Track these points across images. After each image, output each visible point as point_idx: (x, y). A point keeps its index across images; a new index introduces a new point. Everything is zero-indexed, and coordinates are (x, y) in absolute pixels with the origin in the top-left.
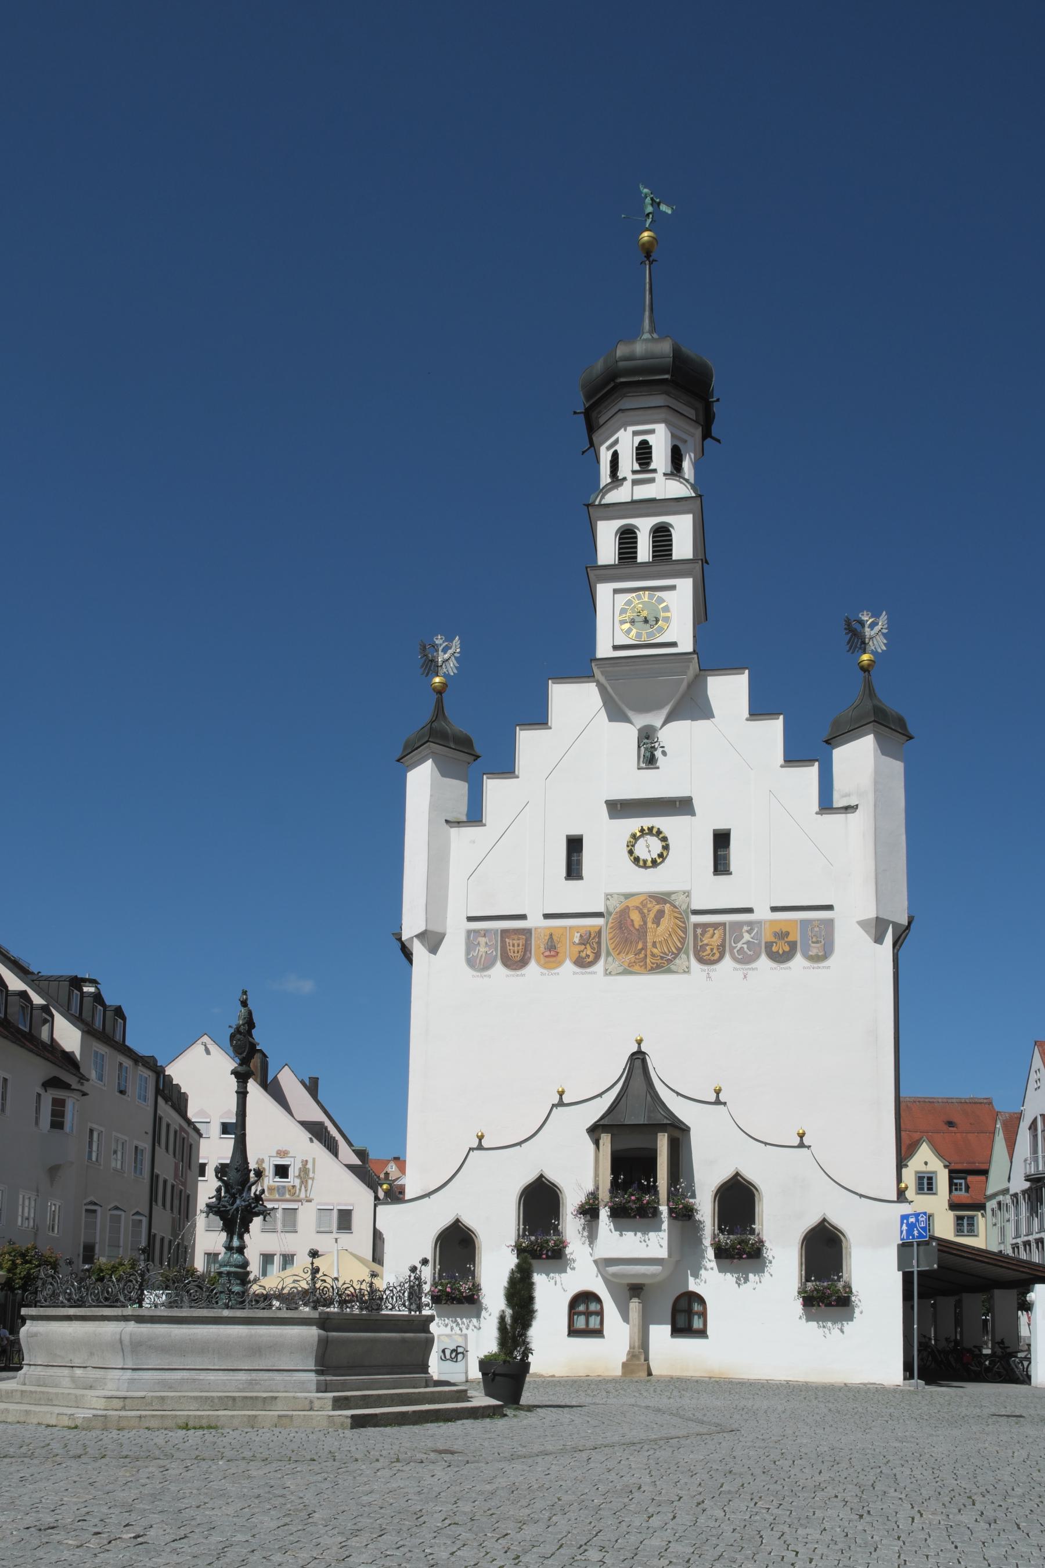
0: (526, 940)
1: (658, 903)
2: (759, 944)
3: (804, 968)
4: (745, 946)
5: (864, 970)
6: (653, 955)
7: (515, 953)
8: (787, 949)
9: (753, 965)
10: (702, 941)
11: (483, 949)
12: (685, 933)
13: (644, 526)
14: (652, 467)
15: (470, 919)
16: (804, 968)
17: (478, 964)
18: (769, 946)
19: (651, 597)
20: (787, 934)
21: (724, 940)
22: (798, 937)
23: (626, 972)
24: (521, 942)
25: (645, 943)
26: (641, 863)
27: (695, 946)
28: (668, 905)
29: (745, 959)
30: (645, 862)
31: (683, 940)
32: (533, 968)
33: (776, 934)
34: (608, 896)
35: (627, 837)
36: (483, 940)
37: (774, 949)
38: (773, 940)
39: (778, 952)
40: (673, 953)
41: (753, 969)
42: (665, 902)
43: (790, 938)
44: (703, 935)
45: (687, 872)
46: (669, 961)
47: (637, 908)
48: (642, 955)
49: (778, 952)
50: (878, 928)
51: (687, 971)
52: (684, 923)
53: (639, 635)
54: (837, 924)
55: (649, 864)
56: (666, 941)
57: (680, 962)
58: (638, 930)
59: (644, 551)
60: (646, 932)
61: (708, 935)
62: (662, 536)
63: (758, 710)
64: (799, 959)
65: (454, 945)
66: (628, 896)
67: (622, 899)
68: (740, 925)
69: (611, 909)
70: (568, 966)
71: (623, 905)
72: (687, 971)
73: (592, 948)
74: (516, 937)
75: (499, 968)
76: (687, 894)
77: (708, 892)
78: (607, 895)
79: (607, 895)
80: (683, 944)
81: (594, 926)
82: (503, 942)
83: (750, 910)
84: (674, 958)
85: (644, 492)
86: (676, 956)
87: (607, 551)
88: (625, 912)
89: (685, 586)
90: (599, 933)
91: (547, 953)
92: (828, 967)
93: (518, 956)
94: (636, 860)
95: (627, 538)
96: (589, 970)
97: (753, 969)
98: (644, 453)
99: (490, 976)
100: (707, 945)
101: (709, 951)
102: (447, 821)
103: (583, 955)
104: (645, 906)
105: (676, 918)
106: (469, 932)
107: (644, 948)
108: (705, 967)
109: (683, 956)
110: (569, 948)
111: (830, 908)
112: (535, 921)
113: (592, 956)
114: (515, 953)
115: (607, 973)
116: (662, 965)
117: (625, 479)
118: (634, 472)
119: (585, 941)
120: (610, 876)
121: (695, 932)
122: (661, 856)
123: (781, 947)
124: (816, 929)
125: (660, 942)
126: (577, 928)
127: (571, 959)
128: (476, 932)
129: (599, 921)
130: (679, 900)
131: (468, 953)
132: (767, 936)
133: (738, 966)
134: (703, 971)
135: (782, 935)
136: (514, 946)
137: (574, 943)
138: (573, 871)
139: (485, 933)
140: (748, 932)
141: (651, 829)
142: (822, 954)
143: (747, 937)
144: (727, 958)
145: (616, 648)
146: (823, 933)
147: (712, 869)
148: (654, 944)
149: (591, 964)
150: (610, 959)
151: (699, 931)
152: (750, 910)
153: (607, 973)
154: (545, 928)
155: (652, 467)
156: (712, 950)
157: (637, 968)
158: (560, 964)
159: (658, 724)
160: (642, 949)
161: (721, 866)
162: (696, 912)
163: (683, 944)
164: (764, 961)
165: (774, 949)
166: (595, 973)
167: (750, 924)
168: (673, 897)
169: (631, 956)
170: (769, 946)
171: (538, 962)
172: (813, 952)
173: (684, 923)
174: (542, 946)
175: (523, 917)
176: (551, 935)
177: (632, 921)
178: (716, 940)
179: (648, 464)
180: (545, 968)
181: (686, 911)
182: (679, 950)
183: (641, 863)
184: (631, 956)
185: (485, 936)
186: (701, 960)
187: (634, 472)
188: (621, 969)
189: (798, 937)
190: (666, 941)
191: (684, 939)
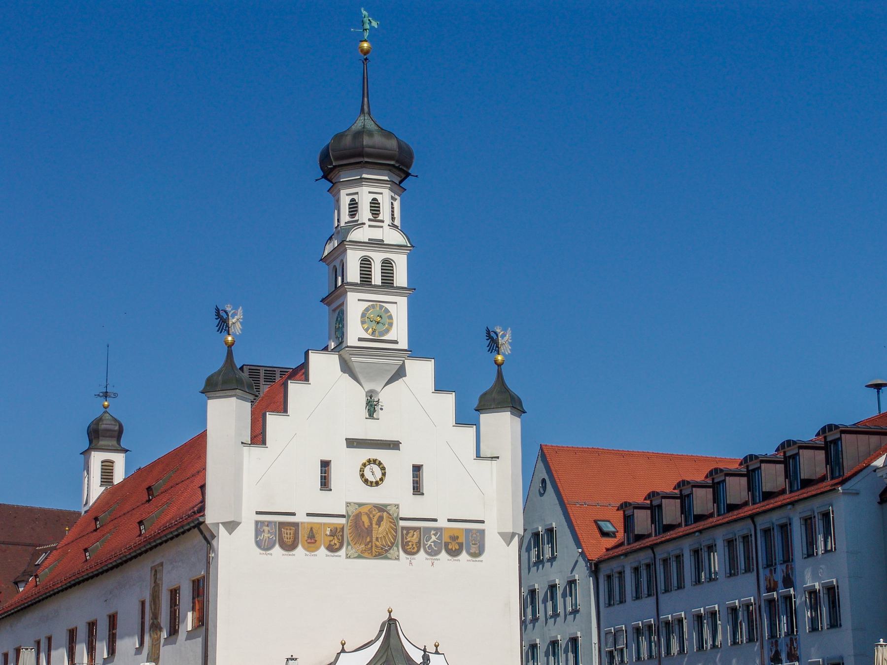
5: (502, 562)
6: (376, 546)
7: (288, 540)
8: (457, 547)
11: (266, 535)
12: (396, 532)
13: (377, 257)
15: (257, 513)
17: (264, 546)
18: (446, 544)
20: (458, 537)
22: (464, 542)
23: (359, 557)
24: (292, 532)
29: (433, 553)
30: (372, 482)
31: (395, 538)
32: (300, 550)
33: (451, 537)
34: (348, 504)
35: (359, 466)
37: (450, 547)
38: (449, 541)
42: (384, 511)
43: (459, 541)
44: (407, 534)
45: (395, 492)
46: (387, 551)
50: (508, 538)
51: (397, 559)
61: (410, 535)
62: (387, 265)
63: (439, 388)
64: (464, 555)
65: (246, 531)
66: (360, 505)
68: (428, 530)
69: (350, 513)
70: (323, 551)
72: (397, 559)
76: (397, 506)
78: (347, 503)
79: (347, 503)
83: (435, 520)
85: (376, 234)
88: (358, 516)
89: (402, 302)
90: (343, 529)
94: (366, 481)
95: (366, 263)
96: (336, 554)
98: (375, 206)
103: (332, 543)
104: (371, 512)
106: (257, 522)
107: (371, 541)
109: (395, 548)
110: (323, 536)
111: (483, 522)
113: (338, 544)
114: (288, 540)
116: (382, 553)
117: (364, 224)
118: (370, 220)
119: (333, 533)
122: (381, 480)
123: (454, 546)
126: (329, 525)
128: (262, 522)
129: (343, 521)
130: (392, 510)
131: (256, 537)
132: (445, 539)
135: (454, 538)
136: (288, 535)
139: (269, 523)
140: (435, 535)
142: (478, 552)
143: (434, 538)
144: (422, 549)
145: (360, 340)
148: (377, 539)
150: (350, 547)
151: (405, 532)
152: (435, 520)
153: (348, 557)
158: (317, 549)
161: (417, 489)
162: (402, 519)
164: (443, 555)
165: (450, 547)
167: (437, 530)
168: (389, 508)
170: (446, 544)
171: (303, 547)
175: (293, 514)
178: (415, 539)
181: (397, 518)
182: (393, 544)
186: (406, 552)
187: (370, 220)
188: (356, 555)
189: (464, 542)
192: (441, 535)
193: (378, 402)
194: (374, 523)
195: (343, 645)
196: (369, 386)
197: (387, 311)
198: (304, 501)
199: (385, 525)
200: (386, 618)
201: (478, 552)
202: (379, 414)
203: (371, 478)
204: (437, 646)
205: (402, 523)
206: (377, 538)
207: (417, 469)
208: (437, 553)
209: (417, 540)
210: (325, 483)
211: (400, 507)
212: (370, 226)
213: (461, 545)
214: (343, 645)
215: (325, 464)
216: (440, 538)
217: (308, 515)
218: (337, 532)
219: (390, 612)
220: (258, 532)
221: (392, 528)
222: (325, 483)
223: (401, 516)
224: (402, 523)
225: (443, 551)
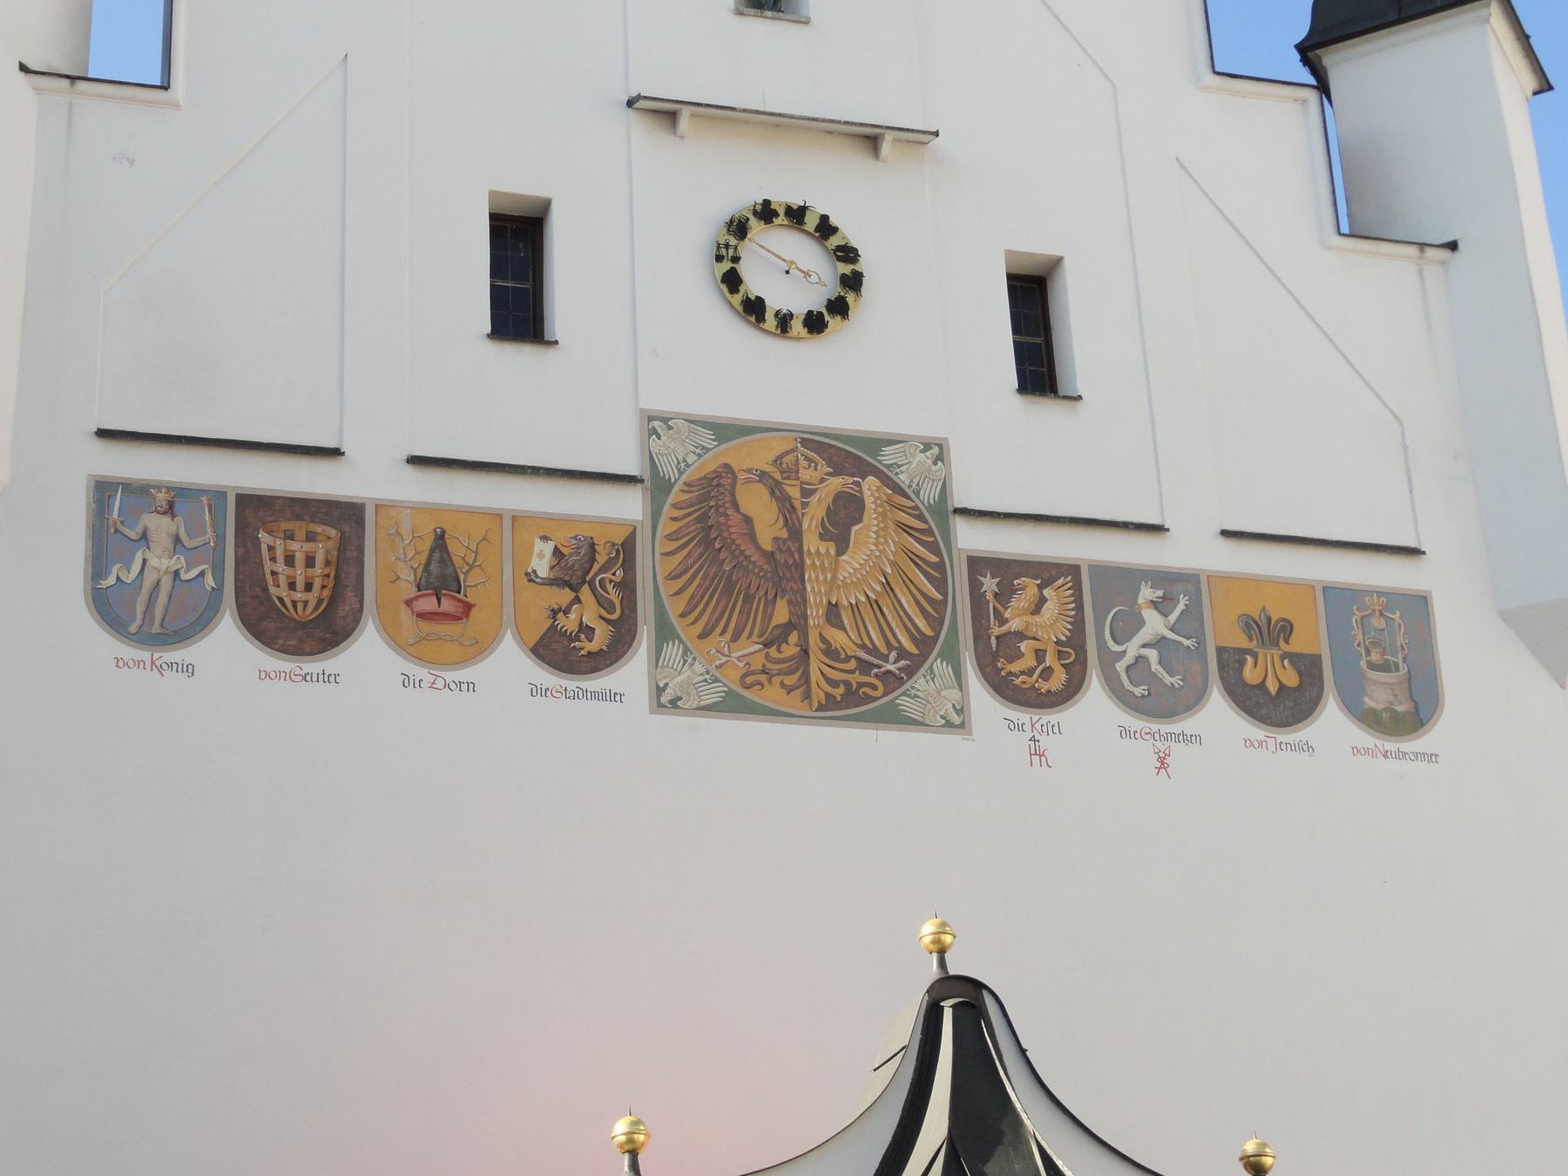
0: (343, 543)
1: (837, 472)
2: (1201, 644)
3: (1356, 751)
4: (1152, 654)
6: (831, 652)
8: (1291, 679)
9: (1188, 725)
10: (1002, 621)
11: (160, 561)
12: (941, 584)
16: (1356, 751)
18: (1231, 661)
20: (1287, 628)
21: (1078, 624)
23: (732, 706)
25: (799, 603)
27: (980, 635)
28: (870, 484)
29: (1158, 702)
30: (784, 321)
31: (936, 611)
32: (368, 653)
33: (1250, 625)
34: (654, 424)
36: (161, 527)
37: (1251, 674)
38: (1243, 643)
39: (1262, 686)
40: (902, 654)
41: (1189, 739)
42: (863, 469)
43: (1298, 645)
44: (1005, 593)
46: (893, 681)
47: (763, 476)
48: (790, 650)
49: (1262, 686)
51: (958, 723)
52: (937, 553)
58: (769, 556)
60: (800, 566)
66: (726, 431)
69: (668, 469)
70: (510, 664)
71: (711, 464)
72: (958, 723)
74: (300, 528)
75: (226, 642)
76: (938, 450)
77: (1004, 460)
80: (936, 624)
81: (604, 523)
84: (911, 671)
88: (715, 490)
90: (627, 549)
91: (428, 604)
92: (1432, 757)
93: (306, 604)
97: (1189, 739)
99: (189, 669)
100: (1021, 636)
101: (1028, 661)
102: (23, 68)
103: (569, 623)
104: (791, 472)
106: (103, 490)
107: (798, 623)
108: (1023, 716)
109: (941, 667)
110: (512, 588)
112: (369, 476)
115: (664, 701)
116: (864, 689)
120: (649, 354)
121: (975, 586)
123: (1269, 670)
124: (1377, 622)
125: (855, 608)
126: (544, 525)
127: (520, 637)
128: (139, 491)
130: (911, 469)
131: (98, 565)
132: (1222, 630)
133: (1135, 723)
134: (1021, 727)
135: (1271, 631)
137: (531, 577)
139: (176, 499)
140: (1162, 606)
141: (796, 215)
142: (1408, 713)
143: (1155, 624)
144: (1095, 688)
146: (1400, 639)
148: (833, 614)
150: (672, 651)
151: (989, 584)
153: (664, 701)
154: (420, 509)
156: (1040, 654)
157: (771, 694)
158: (478, 649)
160: (789, 627)
164: (1217, 714)
165: (1251, 674)
166: (614, 696)
167: (1171, 583)
168: (889, 455)
169: (749, 646)
170: (1231, 661)
171: (392, 635)
172: (1377, 699)
173: (934, 548)
174: (407, 576)
176: (440, 538)
177: (748, 520)
178: (1051, 622)
180: (420, 659)
182: (925, 644)
183: (771, 322)
184: (749, 646)
185: (170, 510)
186: (1003, 688)
188: (712, 695)
190: (875, 605)
191: (940, 605)
198: (395, 395)
199: (872, 542)
200: (933, 972)
201: (1408, 713)
203: (782, 296)
205: (971, 538)
207: (1031, 294)
208: (1190, 701)
210: (519, 311)
211: (955, 454)
213: (1309, 667)
216: (1191, 623)
218: (591, 566)
220: (106, 543)
221: (916, 560)
222: (519, 311)
223: (960, 499)
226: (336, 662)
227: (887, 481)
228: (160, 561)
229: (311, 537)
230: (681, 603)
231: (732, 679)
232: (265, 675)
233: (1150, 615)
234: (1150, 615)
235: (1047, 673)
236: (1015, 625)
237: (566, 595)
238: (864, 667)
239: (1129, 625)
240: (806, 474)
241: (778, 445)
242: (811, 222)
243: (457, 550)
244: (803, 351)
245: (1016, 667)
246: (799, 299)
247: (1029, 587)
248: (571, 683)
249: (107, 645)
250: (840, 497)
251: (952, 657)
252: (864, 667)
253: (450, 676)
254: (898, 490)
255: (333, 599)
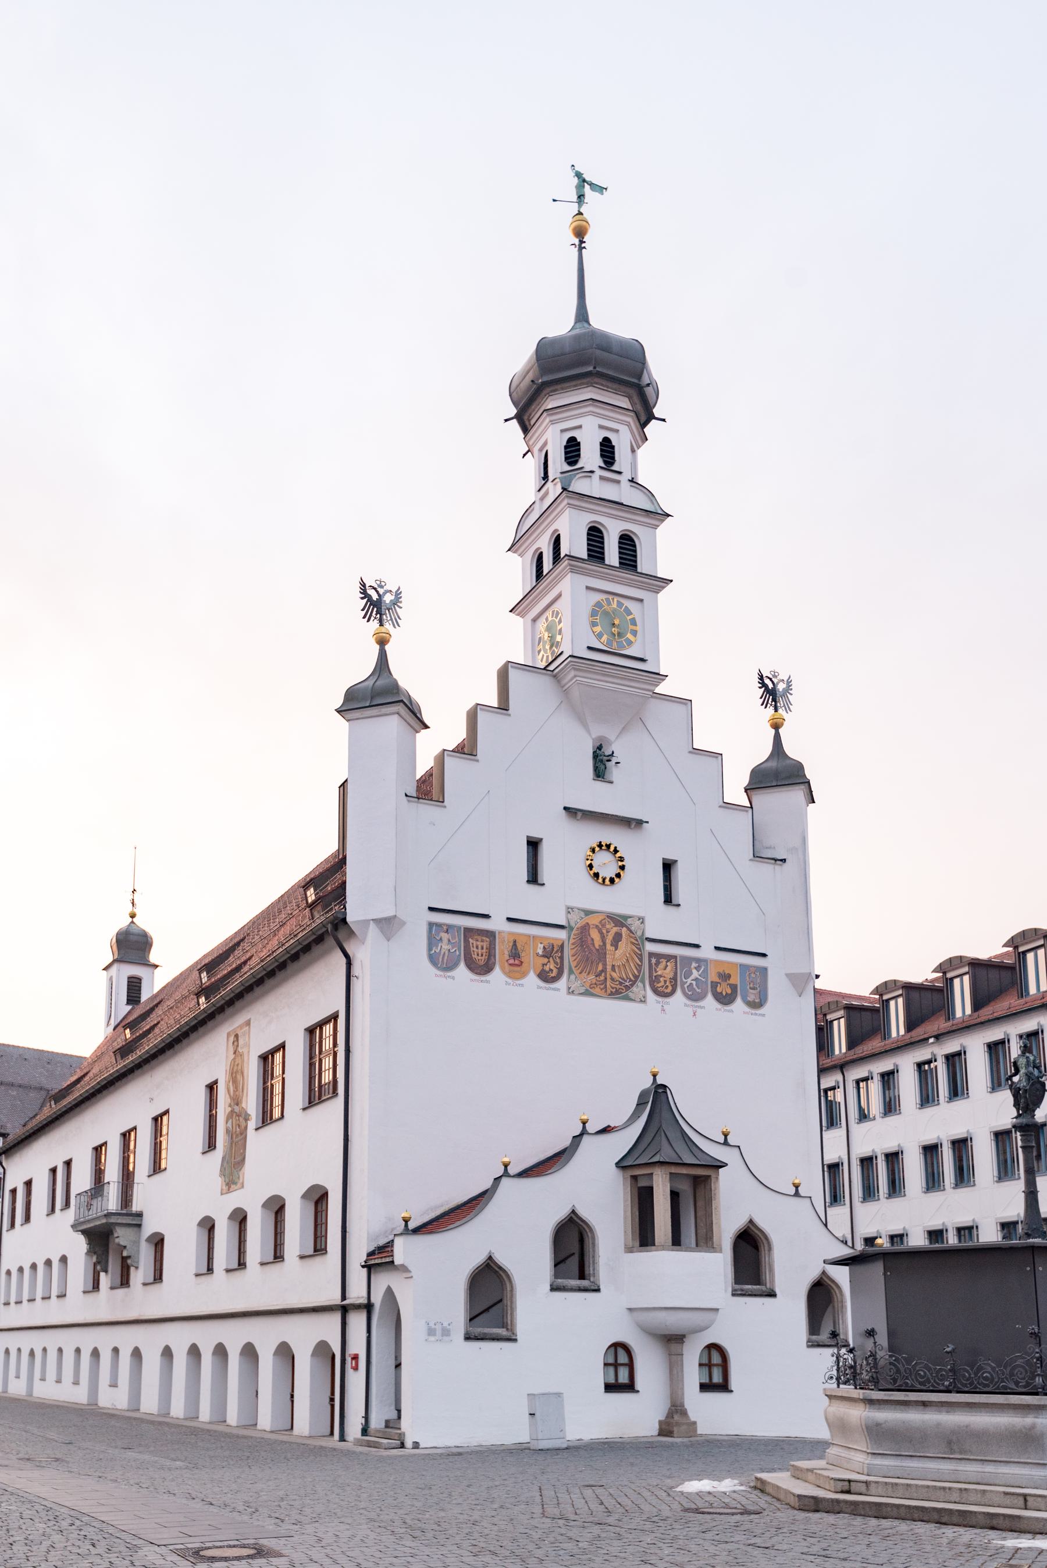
4: (694, 983)
6: (612, 979)
8: (729, 991)
11: (446, 947)
12: (641, 960)
14: (614, 468)
17: (443, 964)
18: (714, 985)
19: (620, 605)
20: (729, 976)
21: (676, 974)
23: (587, 993)
25: (605, 965)
26: (600, 880)
27: (650, 976)
29: (695, 997)
31: (639, 968)
32: (497, 974)
33: (720, 975)
34: (569, 910)
37: (719, 990)
38: (718, 980)
40: (631, 980)
41: (702, 1007)
42: (622, 925)
43: (732, 981)
44: (657, 964)
45: (637, 896)
46: (628, 988)
47: (597, 926)
48: (602, 978)
51: (643, 1001)
53: (609, 643)
54: (770, 972)
55: (607, 882)
56: (624, 965)
57: (637, 990)
59: (612, 554)
60: (605, 954)
61: (662, 966)
64: (739, 1004)
66: (588, 913)
67: (582, 914)
68: (688, 960)
69: (573, 924)
70: (532, 979)
72: (643, 1001)
73: (556, 963)
74: (479, 938)
75: (462, 970)
76: (642, 919)
80: (639, 972)
81: (556, 939)
82: (466, 941)
84: (632, 985)
86: (634, 983)
87: (576, 544)
88: (585, 929)
90: (562, 946)
91: (512, 961)
92: (763, 1015)
93: (481, 960)
95: (595, 535)
97: (702, 1007)
98: (607, 450)
99: (453, 978)
101: (662, 984)
103: (547, 968)
104: (604, 926)
105: (633, 944)
106: (431, 925)
107: (604, 970)
108: (660, 999)
109: (640, 984)
111: (764, 955)
112: (497, 924)
113: (555, 971)
116: (620, 991)
117: (592, 472)
119: (548, 954)
121: (650, 961)
122: (618, 875)
123: (724, 989)
126: (541, 939)
127: (535, 972)
128: (439, 925)
129: (562, 935)
130: (635, 925)
132: (713, 977)
133: (689, 1002)
135: (725, 977)
137: (537, 954)
138: (533, 878)
139: (448, 928)
140: (698, 969)
141: (608, 846)
143: (695, 974)
144: (679, 992)
147: (662, 899)
149: (555, 979)
150: (573, 977)
151: (654, 961)
153: (570, 992)
154: (510, 934)
155: (615, 467)
156: (665, 982)
157: (597, 991)
158: (524, 975)
159: (612, 738)
160: (602, 971)
163: (639, 972)
164: (710, 1000)
165: (719, 990)
166: (558, 990)
170: (714, 985)
172: (751, 998)
173: (639, 949)
174: (506, 953)
178: (668, 973)
179: (612, 464)
180: (510, 977)
182: (636, 977)
183: (600, 880)
185: (447, 932)
186: (656, 991)
188: (582, 990)
189: (737, 984)
190: (624, 965)
192: (706, 971)
193: (612, 754)
194: (608, 942)
195: (584, 1123)
196: (599, 730)
197: (628, 612)
198: (502, 897)
202: (615, 773)
204: (726, 1135)
205: (650, 947)
206: (613, 966)
207: (668, 867)
209: (671, 975)
212: (602, 478)
213: (734, 988)
214: (584, 1123)
215: (534, 845)
217: (509, 919)
218: (553, 952)
219: (655, 1076)
221: (635, 953)
223: (648, 935)
224: (650, 947)
225: (710, 997)
226: (488, 977)
227: (629, 929)
228: (446, 947)
229: (482, 941)
230: (575, 963)
231: (587, 986)
232: (472, 980)
233: (694, 971)
234: (694, 971)
235: (667, 987)
236: (659, 973)
237: (546, 960)
238: (621, 983)
239: (688, 975)
240: (608, 926)
241: (601, 918)
242: (612, 848)
243: (519, 946)
244: (608, 890)
245: (659, 985)
246: (608, 872)
247: (664, 961)
248: (547, 985)
249: (433, 970)
250: (616, 933)
251: (643, 982)
252: (621, 983)
253: (518, 982)
254: (631, 931)
255: (489, 959)
